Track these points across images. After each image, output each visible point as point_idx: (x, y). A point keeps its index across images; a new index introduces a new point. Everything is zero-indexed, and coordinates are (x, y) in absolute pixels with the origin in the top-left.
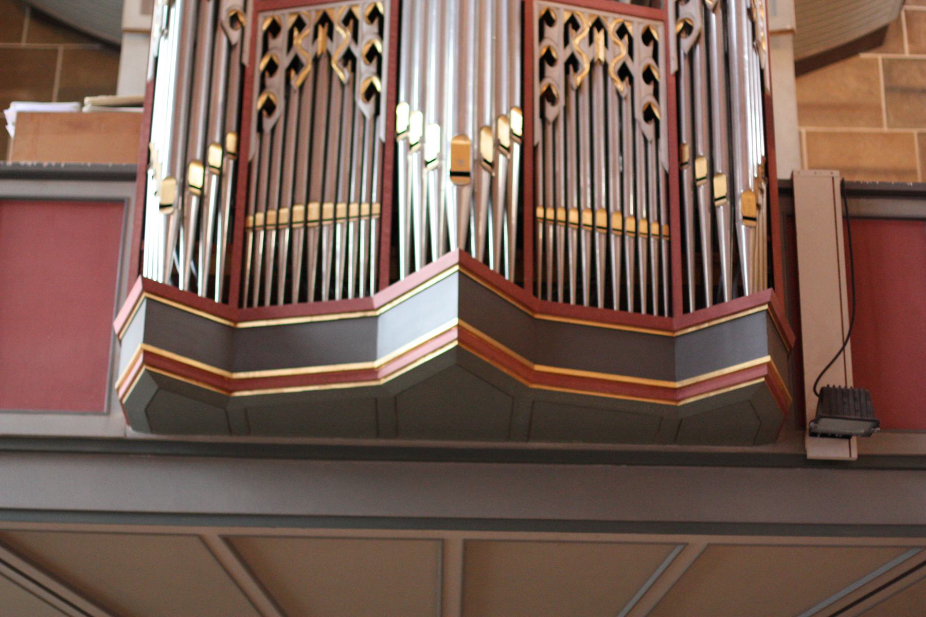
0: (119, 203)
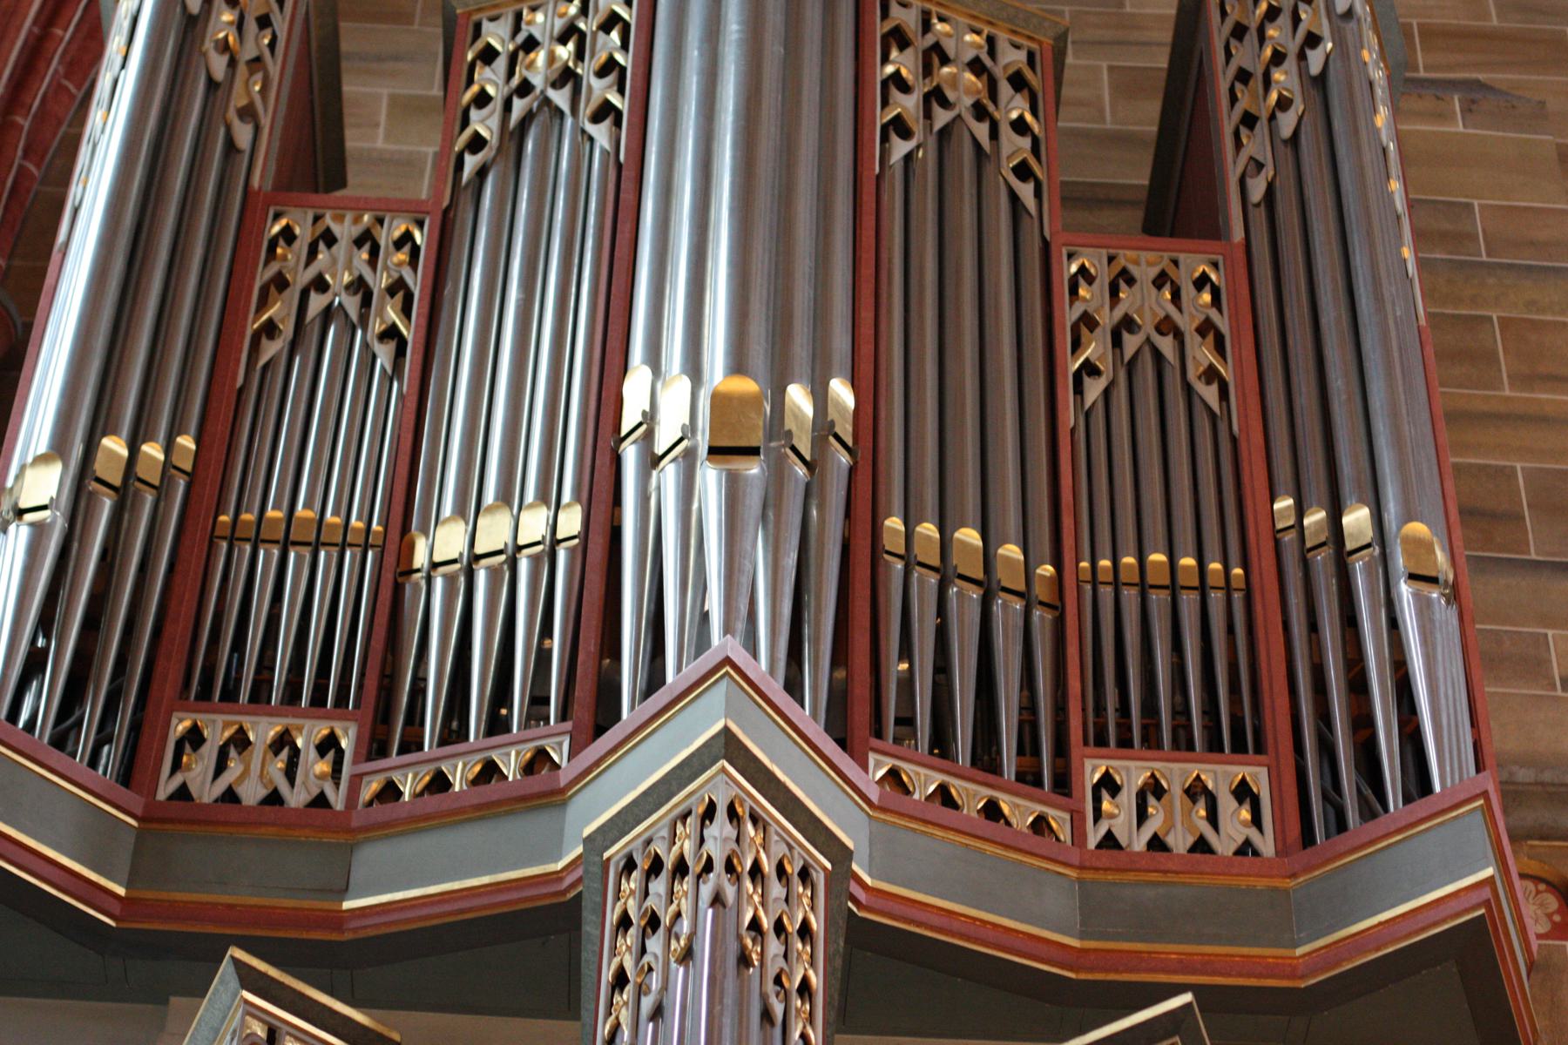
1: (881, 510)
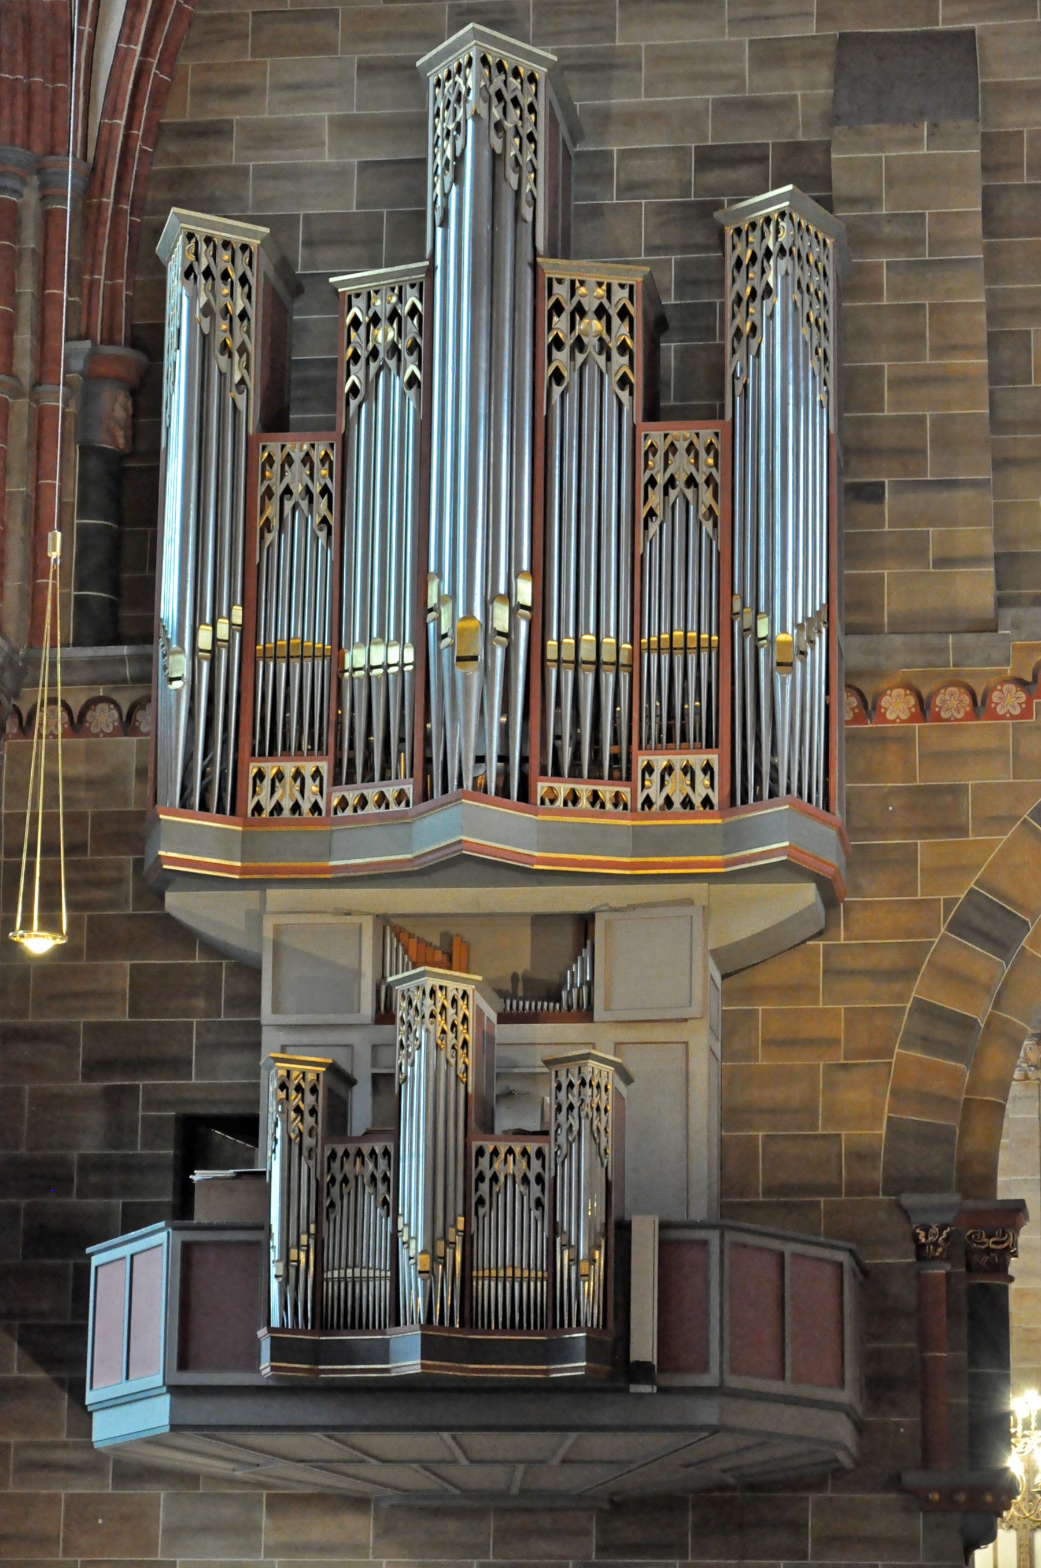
1: (546, 639)
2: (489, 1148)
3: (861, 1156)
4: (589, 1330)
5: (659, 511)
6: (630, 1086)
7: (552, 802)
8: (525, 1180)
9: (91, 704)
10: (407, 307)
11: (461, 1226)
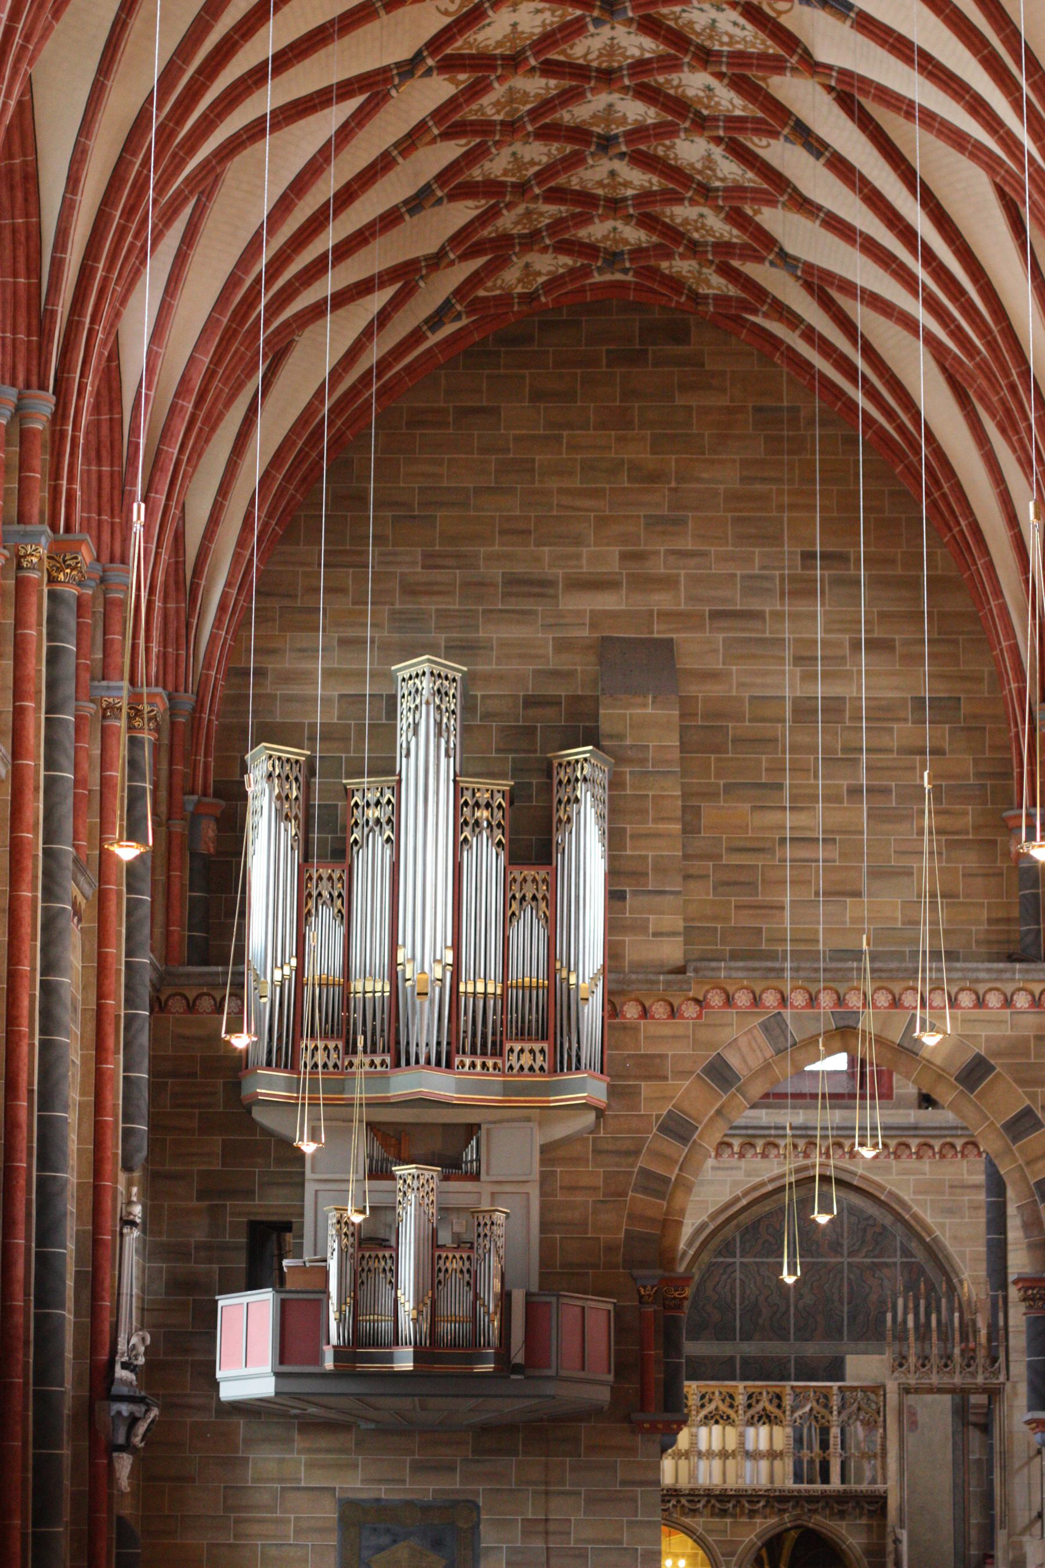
0: (319, 1300)
2: (444, 1255)
3: (610, 1249)
4: (496, 1349)
5: (517, 913)
6: (445, 1183)
7: (463, 1067)
8: (462, 1271)
9: (199, 996)
10: (385, 800)
11: (430, 1295)
